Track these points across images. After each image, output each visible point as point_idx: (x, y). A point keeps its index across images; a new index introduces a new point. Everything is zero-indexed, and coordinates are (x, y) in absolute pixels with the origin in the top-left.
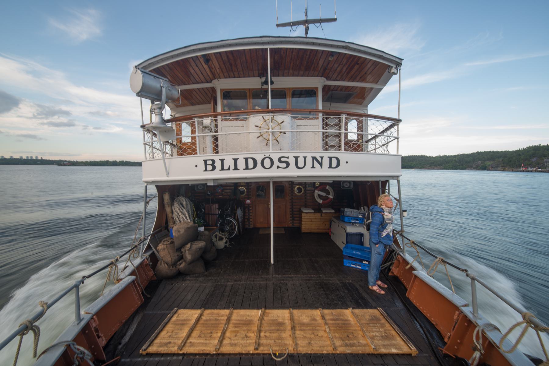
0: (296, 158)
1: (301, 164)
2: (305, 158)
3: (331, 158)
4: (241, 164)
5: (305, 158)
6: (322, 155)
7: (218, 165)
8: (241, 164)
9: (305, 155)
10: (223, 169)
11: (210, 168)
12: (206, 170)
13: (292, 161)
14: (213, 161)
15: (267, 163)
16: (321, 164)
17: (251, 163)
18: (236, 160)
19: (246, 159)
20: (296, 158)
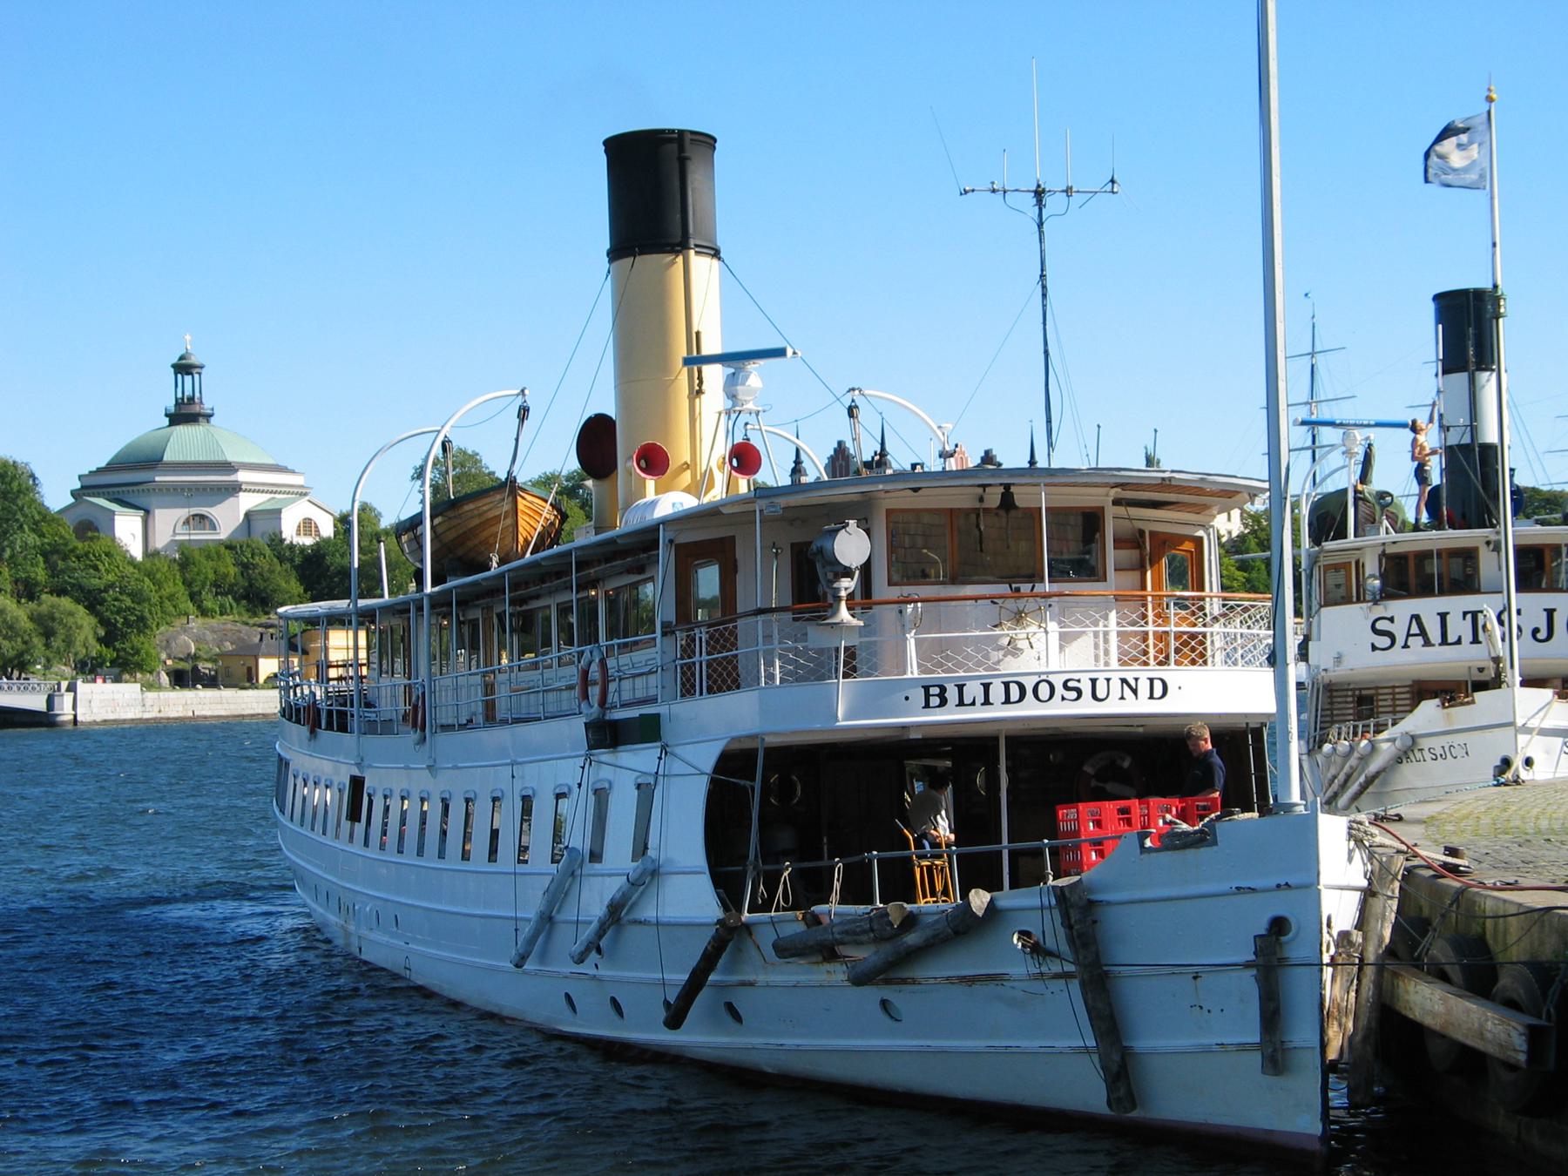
0: (1094, 681)
1: (1101, 693)
2: (1108, 680)
3: (1152, 680)
4: (997, 692)
5: (1108, 680)
6: (1136, 675)
7: (952, 694)
8: (997, 692)
9: (1108, 675)
10: (961, 703)
11: (935, 701)
12: (927, 705)
13: (1086, 687)
14: (943, 689)
15: (1044, 690)
16: (1135, 691)
17: (1015, 692)
18: (986, 687)
19: (1007, 685)
20: (1094, 681)
